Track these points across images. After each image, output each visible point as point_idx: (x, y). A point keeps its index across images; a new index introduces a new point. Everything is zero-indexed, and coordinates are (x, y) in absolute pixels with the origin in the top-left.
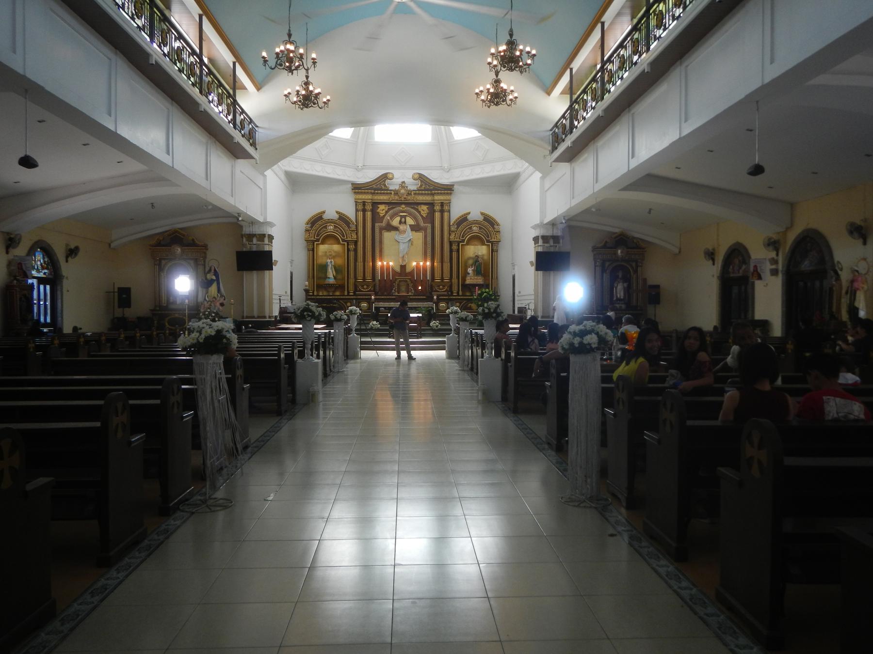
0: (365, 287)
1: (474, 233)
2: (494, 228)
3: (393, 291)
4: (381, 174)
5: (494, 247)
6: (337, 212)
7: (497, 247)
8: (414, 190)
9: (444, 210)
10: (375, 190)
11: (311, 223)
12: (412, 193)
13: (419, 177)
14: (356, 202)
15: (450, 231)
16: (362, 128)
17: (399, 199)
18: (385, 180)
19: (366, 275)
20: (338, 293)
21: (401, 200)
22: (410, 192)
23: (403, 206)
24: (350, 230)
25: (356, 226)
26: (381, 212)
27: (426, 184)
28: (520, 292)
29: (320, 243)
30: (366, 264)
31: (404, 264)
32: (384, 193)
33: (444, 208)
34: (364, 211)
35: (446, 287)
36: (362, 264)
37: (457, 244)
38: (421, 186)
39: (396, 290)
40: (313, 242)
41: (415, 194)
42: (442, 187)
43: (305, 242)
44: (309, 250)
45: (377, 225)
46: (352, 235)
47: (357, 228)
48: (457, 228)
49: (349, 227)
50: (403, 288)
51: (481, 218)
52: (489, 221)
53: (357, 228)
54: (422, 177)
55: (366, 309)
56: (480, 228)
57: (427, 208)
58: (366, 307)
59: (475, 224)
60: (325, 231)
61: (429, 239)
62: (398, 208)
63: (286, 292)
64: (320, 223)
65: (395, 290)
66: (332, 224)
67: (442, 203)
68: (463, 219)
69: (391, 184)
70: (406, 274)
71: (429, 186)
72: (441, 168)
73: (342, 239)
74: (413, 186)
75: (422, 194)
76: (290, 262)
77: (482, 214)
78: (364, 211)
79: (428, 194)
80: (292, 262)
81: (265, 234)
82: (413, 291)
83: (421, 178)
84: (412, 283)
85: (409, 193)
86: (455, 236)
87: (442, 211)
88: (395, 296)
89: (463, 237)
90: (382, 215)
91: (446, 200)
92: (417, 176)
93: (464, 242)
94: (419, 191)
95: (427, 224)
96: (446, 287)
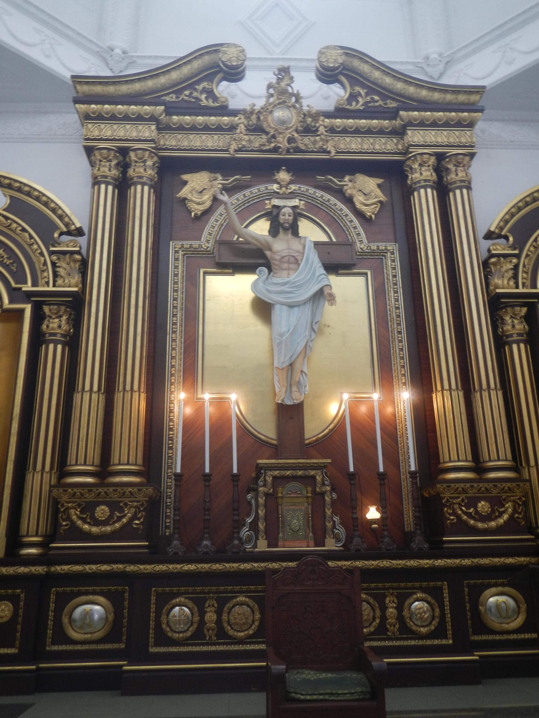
0: (102, 511)
3: (245, 532)
8: (328, 115)
10: (170, 110)
13: (344, 69)
14: (89, 151)
21: (276, 150)
23: (283, 176)
24: (51, 253)
26: (195, 198)
27: (371, 91)
30: (118, 397)
31: (297, 397)
32: (206, 128)
35: (509, 505)
37: (524, 310)
38: (353, 97)
39: (261, 526)
46: (61, 272)
48: (520, 244)
49: (48, 241)
57: (379, 186)
62: (262, 187)
65: (254, 526)
67: (440, 157)
71: (384, 97)
73: (11, 291)
75: (357, 132)
79: (381, 132)
82: (341, 531)
84: (333, 489)
86: (515, 277)
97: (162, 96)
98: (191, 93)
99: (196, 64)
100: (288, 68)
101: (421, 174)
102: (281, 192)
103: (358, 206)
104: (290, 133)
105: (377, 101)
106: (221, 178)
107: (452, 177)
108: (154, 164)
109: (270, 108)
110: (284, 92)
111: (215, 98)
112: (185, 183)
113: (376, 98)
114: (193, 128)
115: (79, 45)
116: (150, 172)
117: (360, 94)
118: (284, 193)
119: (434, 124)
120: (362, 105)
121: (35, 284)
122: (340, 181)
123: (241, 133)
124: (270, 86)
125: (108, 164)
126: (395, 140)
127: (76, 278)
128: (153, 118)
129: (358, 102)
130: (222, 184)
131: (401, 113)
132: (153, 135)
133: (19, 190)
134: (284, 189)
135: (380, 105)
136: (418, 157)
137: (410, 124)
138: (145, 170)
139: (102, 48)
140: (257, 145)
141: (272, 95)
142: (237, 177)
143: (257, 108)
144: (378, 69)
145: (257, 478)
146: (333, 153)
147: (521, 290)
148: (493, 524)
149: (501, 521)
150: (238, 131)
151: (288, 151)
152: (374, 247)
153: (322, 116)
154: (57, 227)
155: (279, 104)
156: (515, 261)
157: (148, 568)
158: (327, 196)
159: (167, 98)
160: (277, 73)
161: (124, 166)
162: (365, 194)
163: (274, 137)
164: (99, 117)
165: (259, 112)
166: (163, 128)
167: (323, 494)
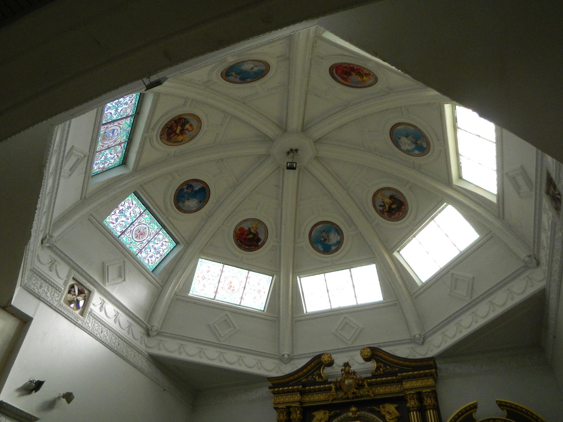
9: (426, 406)
10: (304, 385)
14: (276, 408)
21: (348, 398)
23: (353, 409)
27: (385, 365)
32: (320, 391)
38: (378, 368)
57: (396, 408)
62: (345, 415)
69: (332, 376)
71: (391, 367)
72: (413, 341)
75: (382, 384)
77: (501, 405)
79: (392, 382)
85: (360, 386)
92: (368, 353)
97: (301, 380)
98: (312, 376)
100: (348, 362)
101: (410, 404)
102: (353, 416)
103: (387, 420)
104: (353, 390)
105: (389, 369)
106: (328, 412)
107: (426, 403)
108: (300, 412)
109: (343, 379)
112: (314, 416)
113: (388, 367)
115: (272, 358)
116: (299, 416)
117: (381, 367)
118: (355, 417)
119: (414, 377)
120: (382, 372)
122: (378, 408)
123: (333, 392)
124: (342, 370)
125: (282, 415)
126: (400, 386)
128: (298, 390)
129: (380, 370)
130: (329, 416)
131: (398, 374)
132: (299, 398)
134: (354, 415)
135: (390, 370)
136: (408, 396)
137: (403, 378)
138: (296, 416)
139: (280, 356)
140: (341, 395)
141: (343, 374)
142: (334, 412)
143: (339, 380)
144: (386, 355)
146: (373, 396)
150: (332, 391)
151: (353, 398)
153: (366, 379)
155: (346, 378)
158: (374, 416)
159: (303, 380)
160: (343, 365)
161: (289, 413)
162: (390, 414)
163: (346, 392)
165: (339, 381)
166: (302, 393)
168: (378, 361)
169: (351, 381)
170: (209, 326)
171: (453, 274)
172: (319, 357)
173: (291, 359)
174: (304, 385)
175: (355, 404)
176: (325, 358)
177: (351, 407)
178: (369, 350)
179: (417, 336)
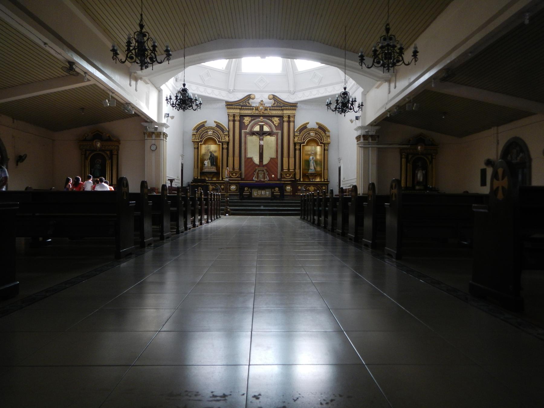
0: (234, 174)
1: (311, 137)
2: (325, 134)
3: (254, 178)
4: (246, 96)
5: (326, 147)
6: (215, 122)
7: (328, 147)
8: (269, 107)
10: (242, 107)
11: (196, 129)
12: (268, 109)
14: (228, 115)
15: (294, 135)
16: (234, 60)
17: (259, 113)
18: (249, 99)
19: (235, 167)
20: (215, 179)
21: (260, 114)
22: (266, 108)
23: (262, 118)
25: (228, 131)
26: (246, 122)
27: (278, 103)
28: (344, 179)
29: (202, 143)
32: (248, 109)
33: (290, 120)
34: (234, 121)
35: (292, 175)
36: (232, 158)
37: (299, 145)
38: (274, 104)
40: (198, 143)
41: (270, 109)
42: (289, 104)
43: (192, 142)
44: (195, 148)
45: (243, 131)
47: (229, 133)
48: (300, 133)
49: (223, 132)
50: (261, 176)
51: (316, 127)
52: (322, 128)
53: (229, 133)
54: (276, 98)
55: (235, 190)
56: (316, 134)
57: (279, 119)
58: (235, 188)
59: (312, 131)
60: (206, 135)
61: (280, 141)
63: (178, 177)
64: (202, 129)
65: (255, 177)
66: (211, 130)
68: (304, 127)
70: (264, 166)
71: (280, 104)
72: (289, 92)
74: (269, 103)
75: (275, 110)
76: (181, 156)
77: (317, 124)
78: (234, 121)
79: (279, 110)
80: (183, 156)
81: (160, 133)
82: (268, 178)
83: (274, 98)
84: (267, 172)
85: (266, 109)
86: (298, 139)
87: (289, 122)
88: (254, 181)
89: (304, 140)
90: (246, 124)
91: (293, 114)
92: (272, 97)
93: (304, 144)
94: (272, 108)
95: (278, 131)
96: (292, 175)
99: (246, 98)
110: (262, 104)
111: (250, 104)
112: (244, 119)
114: (246, 109)
119: (288, 109)
121: (222, 140)
124: (259, 102)
127: (228, 139)
128: (239, 108)
133: (218, 123)
137: (284, 109)
143: (257, 106)
145: (256, 170)
147: (298, 142)
148: (289, 178)
149: (290, 177)
151: (262, 114)
152: (277, 131)
154: (224, 130)
156: (298, 136)
157: (241, 182)
159: (241, 104)
161: (234, 117)
164: (230, 108)
166: (240, 109)
167: (265, 173)
168: (275, 101)
169: (262, 107)
170: (200, 76)
171: (315, 72)
172: (250, 95)
173: (233, 92)
174: (242, 107)
175: (263, 116)
176: (252, 96)
177: (261, 117)
178: (272, 96)
179: (292, 91)
